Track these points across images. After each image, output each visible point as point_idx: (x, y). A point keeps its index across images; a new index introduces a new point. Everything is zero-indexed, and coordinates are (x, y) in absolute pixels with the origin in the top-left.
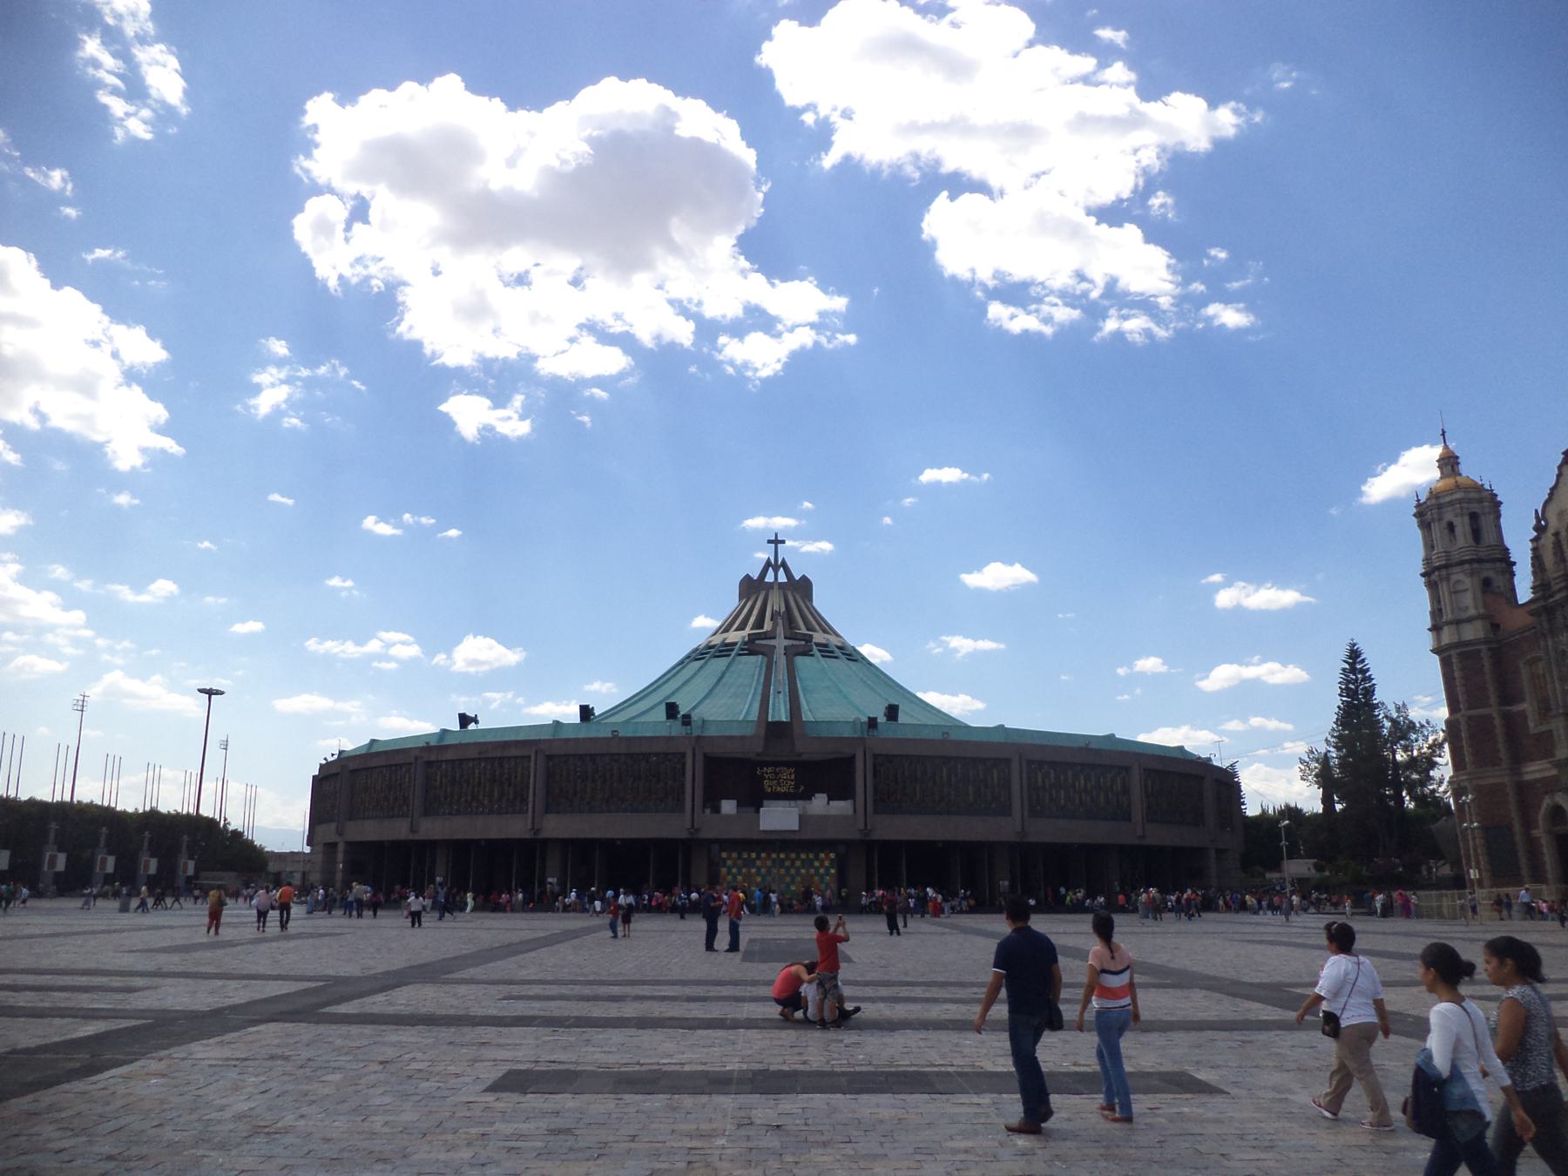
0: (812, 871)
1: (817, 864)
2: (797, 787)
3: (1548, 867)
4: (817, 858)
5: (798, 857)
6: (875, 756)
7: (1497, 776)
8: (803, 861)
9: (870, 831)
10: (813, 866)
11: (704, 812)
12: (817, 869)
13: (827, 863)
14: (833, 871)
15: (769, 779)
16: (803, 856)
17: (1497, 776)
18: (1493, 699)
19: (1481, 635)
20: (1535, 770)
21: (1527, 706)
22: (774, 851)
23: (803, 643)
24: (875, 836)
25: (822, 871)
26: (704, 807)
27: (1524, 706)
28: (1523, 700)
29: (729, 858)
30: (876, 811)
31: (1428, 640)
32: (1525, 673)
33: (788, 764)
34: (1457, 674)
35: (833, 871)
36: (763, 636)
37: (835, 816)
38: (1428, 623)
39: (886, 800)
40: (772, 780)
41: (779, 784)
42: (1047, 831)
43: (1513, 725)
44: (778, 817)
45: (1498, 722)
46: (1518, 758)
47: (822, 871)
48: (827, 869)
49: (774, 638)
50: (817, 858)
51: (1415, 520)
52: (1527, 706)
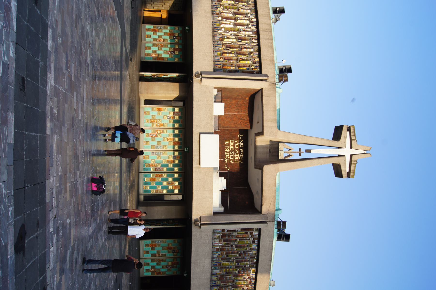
0: (165, 176)
1: (170, 179)
2: (229, 164)
4: (175, 180)
6: (259, 230)
8: (173, 169)
9: (200, 227)
10: (169, 176)
11: (215, 88)
12: (167, 180)
13: (171, 187)
14: (165, 192)
15: (235, 143)
16: (176, 169)
22: (179, 147)
23: (348, 171)
24: (195, 230)
25: (165, 183)
26: (220, 90)
36: (353, 138)
37: (212, 198)
40: (234, 146)
41: (232, 151)
47: (165, 183)
48: (166, 187)
49: (351, 148)
50: (175, 180)
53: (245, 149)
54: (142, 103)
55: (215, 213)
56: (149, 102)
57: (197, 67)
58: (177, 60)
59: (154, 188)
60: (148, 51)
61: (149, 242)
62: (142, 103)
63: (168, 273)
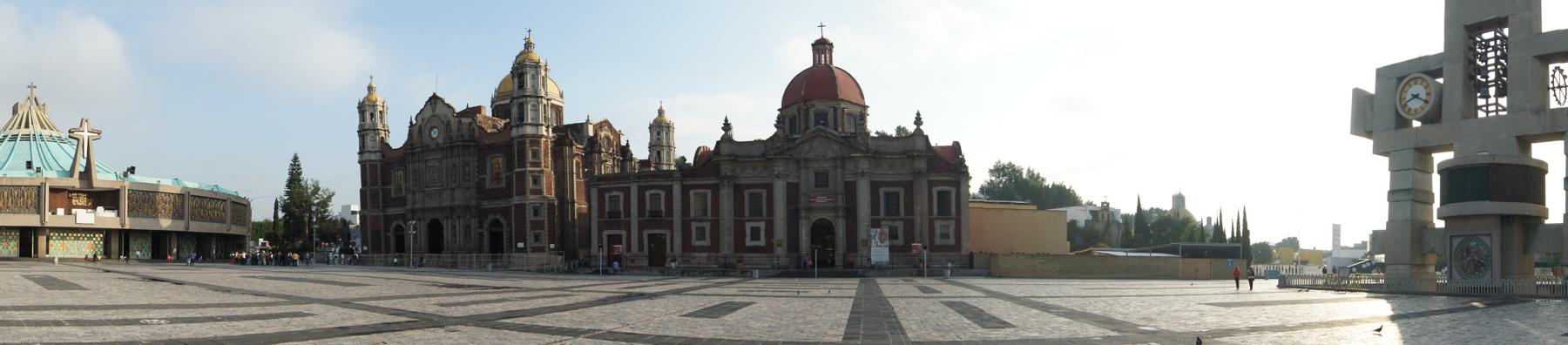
3: (392, 247)
4: (94, 236)
5: (86, 236)
7: (378, 213)
17: (378, 213)
18: (380, 184)
19: (378, 158)
20: (391, 211)
21: (392, 187)
27: (390, 187)
28: (390, 183)
29: (54, 235)
30: (129, 216)
31: (357, 158)
32: (393, 176)
33: (84, 192)
34: (368, 172)
35: (101, 243)
38: (358, 151)
39: (133, 211)
42: (196, 227)
43: (386, 193)
44: (85, 217)
45: (380, 192)
46: (386, 206)
51: (357, 110)
52: (392, 187)
53: (78, 192)
54: (47, 256)
55: (118, 216)
56: (47, 253)
57: (39, 225)
58: (18, 234)
59: (99, 250)
60: (12, 252)
61: (131, 253)
62: (47, 256)
63: (150, 241)
